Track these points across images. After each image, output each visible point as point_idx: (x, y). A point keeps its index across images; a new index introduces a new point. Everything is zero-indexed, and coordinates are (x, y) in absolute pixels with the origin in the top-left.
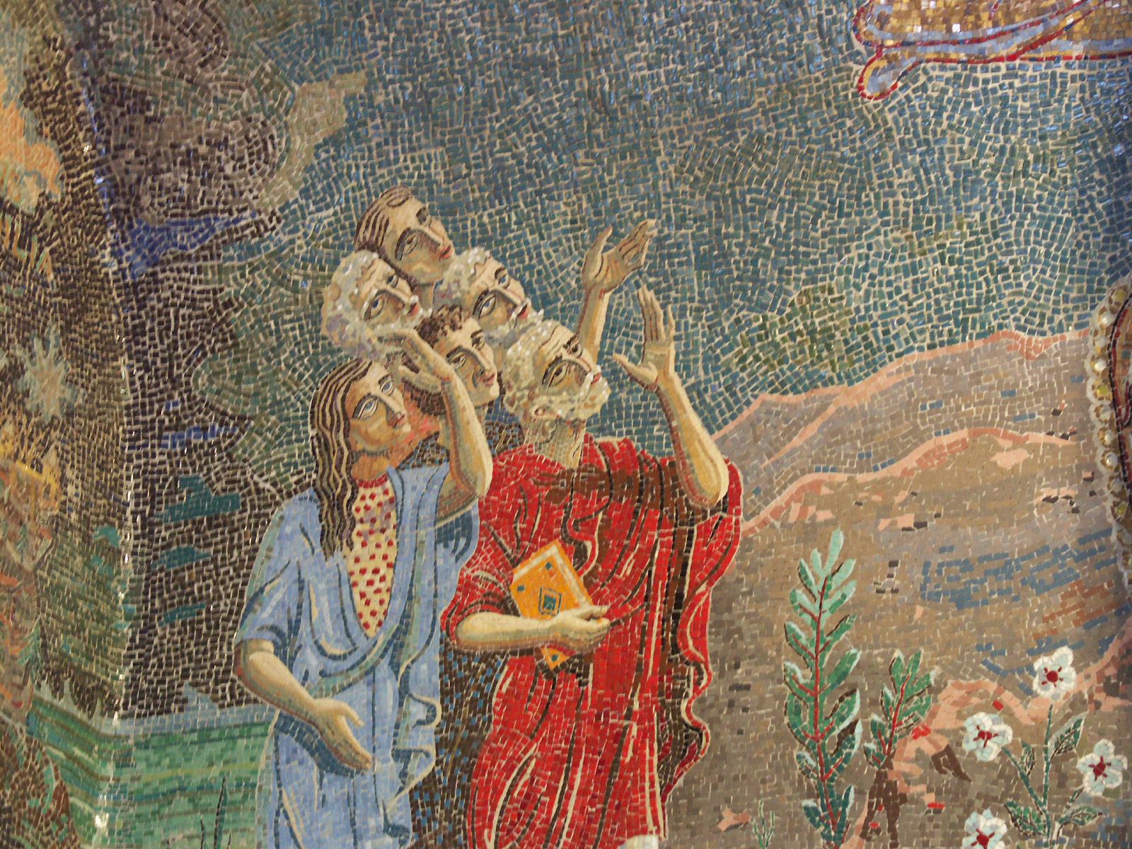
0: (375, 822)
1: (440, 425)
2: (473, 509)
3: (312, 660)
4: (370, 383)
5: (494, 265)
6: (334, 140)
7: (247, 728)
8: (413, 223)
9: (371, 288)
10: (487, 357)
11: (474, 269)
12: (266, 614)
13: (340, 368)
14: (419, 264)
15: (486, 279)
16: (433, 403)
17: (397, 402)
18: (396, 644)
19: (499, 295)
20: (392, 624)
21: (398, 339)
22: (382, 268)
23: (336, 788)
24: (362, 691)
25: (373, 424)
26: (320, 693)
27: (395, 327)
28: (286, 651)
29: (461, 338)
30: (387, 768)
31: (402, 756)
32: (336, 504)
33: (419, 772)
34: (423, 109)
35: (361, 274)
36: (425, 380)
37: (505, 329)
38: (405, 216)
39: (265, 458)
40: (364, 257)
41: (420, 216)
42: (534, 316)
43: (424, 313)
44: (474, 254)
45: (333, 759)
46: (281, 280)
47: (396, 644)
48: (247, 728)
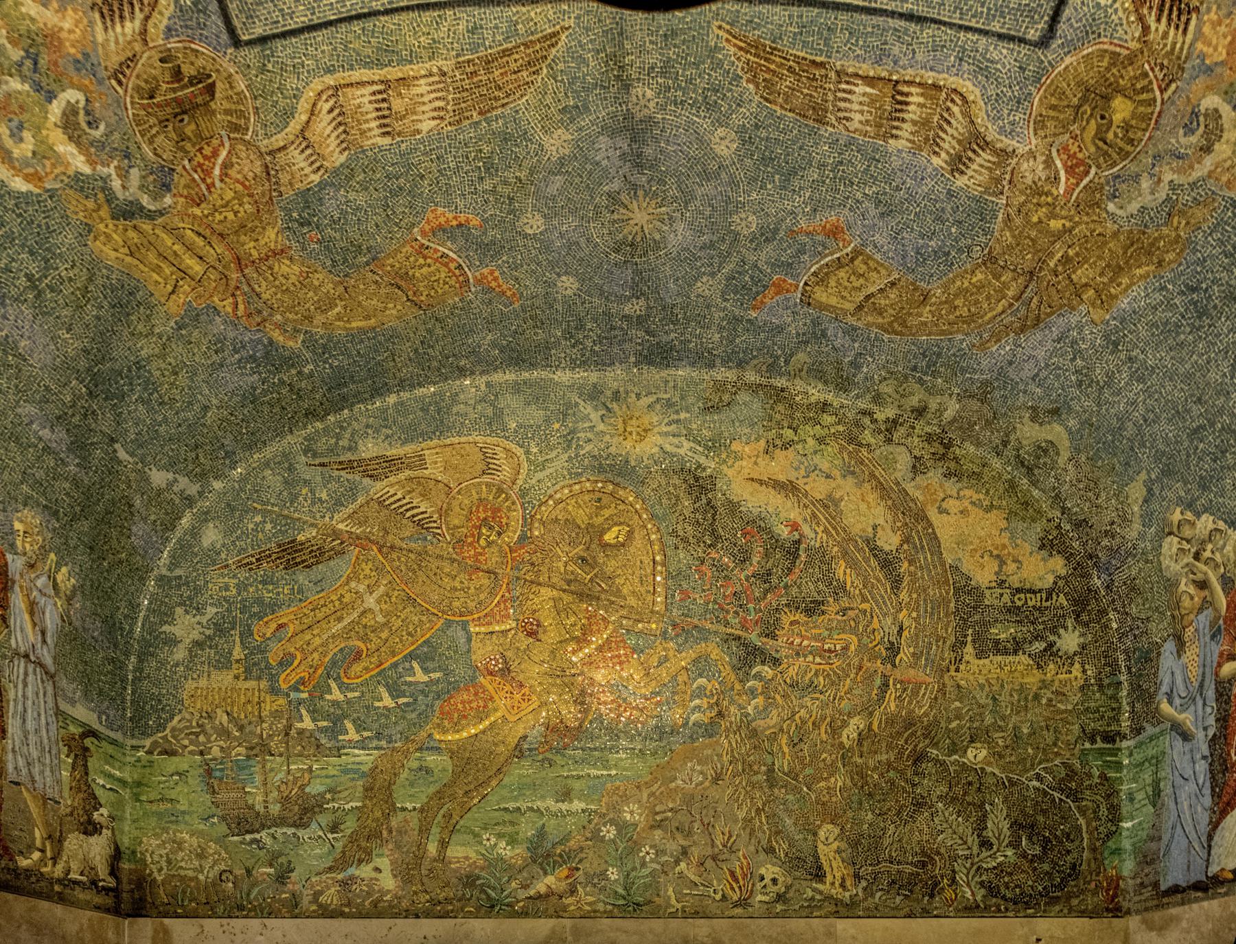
0: (1198, 756)
1: (1206, 592)
2: (1221, 622)
3: (1177, 701)
4: (1182, 587)
5: (1211, 518)
6: (1146, 501)
7: (1162, 733)
8: (1181, 517)
9: (1174, 550)
10: (1218, 557)
11: (1206, 523)
12: (1165, 688)
13: (1171, 585)
14: (1187, 532)
15: (1211, 526)
16: (1203, 585)
17: (1192, 590)
18: (1201, 686)
19: (1216, 530)
20: (1200, 679)
21: (1187, 565)
22: (1176, 540)
23: (1188, 746)
24: (1192, 708)
25: (1186, 603)
26: (1181, 712)
27: (1185, 561)
28: (1170, 702)
29: (1207, 554)
30: (1200, 735)
31: (1205, 729)
32: (1179, 639)
33: (1211, 733)
34: (1167, 472)
35: (1171, 545)
36: (1199, 577)
37: (1221, 542)
38: (1177, 516)
39: (1158, 629)
40: (1169, 539)
41: (1182, 513)
42: (1230, 531)
43: (1193, 550)
44: (1204, 517)
45: (1186, 736)
46: (1147, 562)
47: (1201, 686)
48: (1162, 733)
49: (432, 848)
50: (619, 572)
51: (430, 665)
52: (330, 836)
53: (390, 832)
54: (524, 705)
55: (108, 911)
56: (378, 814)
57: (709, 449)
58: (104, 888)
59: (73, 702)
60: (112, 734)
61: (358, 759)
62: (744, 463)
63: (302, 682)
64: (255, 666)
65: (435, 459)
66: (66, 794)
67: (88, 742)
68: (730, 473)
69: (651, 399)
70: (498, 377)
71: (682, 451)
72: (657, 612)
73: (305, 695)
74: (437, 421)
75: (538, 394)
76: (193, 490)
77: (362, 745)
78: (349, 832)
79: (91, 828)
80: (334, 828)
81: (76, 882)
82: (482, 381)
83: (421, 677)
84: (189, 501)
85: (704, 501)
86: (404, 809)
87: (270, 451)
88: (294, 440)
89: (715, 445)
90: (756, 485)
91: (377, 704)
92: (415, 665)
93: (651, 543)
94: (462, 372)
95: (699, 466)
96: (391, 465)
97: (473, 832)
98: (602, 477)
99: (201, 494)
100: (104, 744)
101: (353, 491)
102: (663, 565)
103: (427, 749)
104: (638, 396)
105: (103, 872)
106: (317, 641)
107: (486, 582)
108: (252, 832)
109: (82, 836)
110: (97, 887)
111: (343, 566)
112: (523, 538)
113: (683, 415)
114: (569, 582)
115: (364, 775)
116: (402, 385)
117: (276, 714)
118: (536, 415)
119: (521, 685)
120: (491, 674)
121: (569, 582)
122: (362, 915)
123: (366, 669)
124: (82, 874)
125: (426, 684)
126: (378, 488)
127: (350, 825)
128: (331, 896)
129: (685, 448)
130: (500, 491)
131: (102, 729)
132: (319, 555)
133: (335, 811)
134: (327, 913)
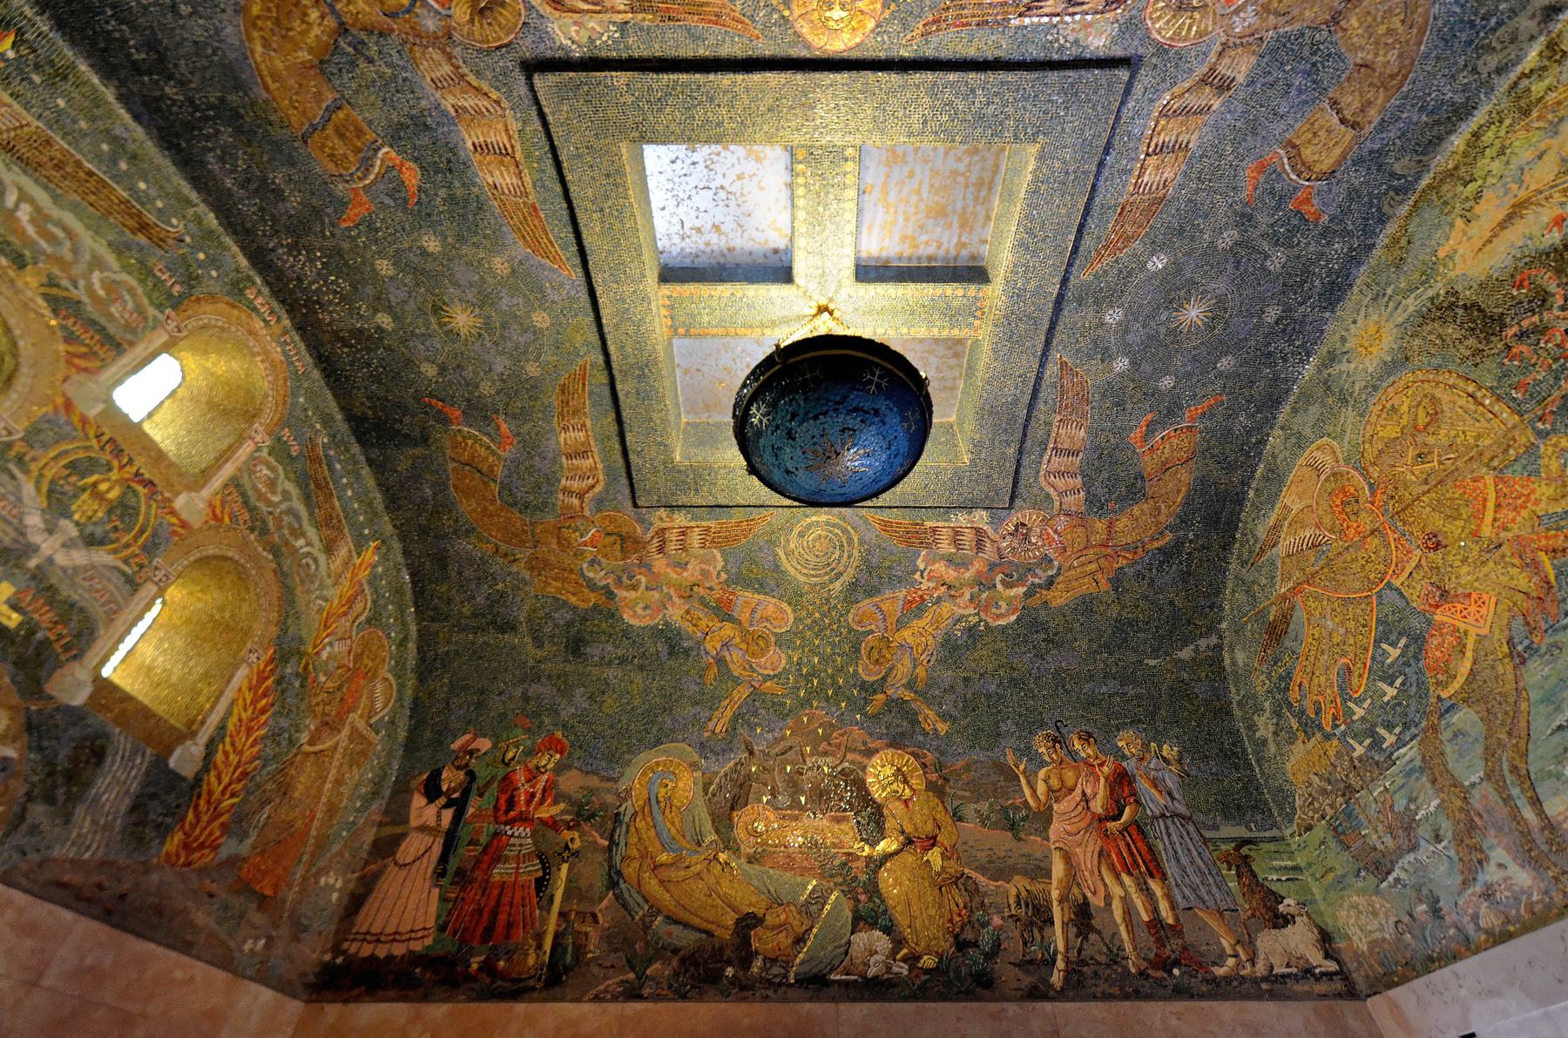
49: (1529, 814)
50: (1453, 433)
51: (1393, 638)
52: (1440, 847)
53: (1481, 817)
54: (1484, 611)
55: (1340, 996)
56: (1459, 803)
57: (1427, 281)
58: (1323, 974)
59: (1216, 827)
60: (1267, 834)
61: (1407, 758)
62: (1461, 251)
63: (1335, 718)
64: (1310, 727)
65: (1291, 499)
66: (1240, 900)
67: (1245, 851)
68: (1458, 272)
69: (1362, 313)
70: (1281, 418)
71: (1412, 309)
72: (1514, 427)
73: (1343, 727)
74: (1276, 478)
75: (1306, 398)
76: (1214, 640)
77: (1401, 743)
78: (1450, 834)
79: (1283, 922)
80: (1438, 838)
81: (1283, 976)
82: (1277, 432)
83: (1395, 653)
84: (1219, 647)
85: (1460, 312)
86: (1473, 785)
87: (1230, 584)
88: (1234, 565)
89: (1428, 275)
90: (1489, 247)
91: (1386, 699)
92: (1384, 646)
93: (1452, 387)
94: (1262, 442)
95: (1432, 299)
96: (1276, 528)
97: (1550, 774)
98: (1381, 391)
99: (1221, 638)
100: (1262, 845)
101: (1273, 564)
102: (1480, 388)
103: (1447, 711)
104: (1354, 322)
105: (1316, 958)
106: (1323, 679)
107: (1376, 541)
108: (1389, 873)
109: (1273, 932)
110: (1313, 975)
111: (1300, 615)
112: (1371, 486)
113: (1389, 291)
114: (1426, 482)
115: (1422, 769)
116: (1245, 483)
117: (1339, 755)
118: (1314, 410)
119: (1469, 595)
120: (1437, 606)
121: (1426, 482)
122: (1527, 928)
123: (1360, 676)
124: (1288, 966)
125: (1403, 654)
126: (1281, 549)
127: (1446, 827)
128: (1489, 919)
129: (1412, 304)
130: (1334, 474)
131: (1253, 835)
132: (1286, 618)
133: (1426, 818)
134: (1500, 937)
